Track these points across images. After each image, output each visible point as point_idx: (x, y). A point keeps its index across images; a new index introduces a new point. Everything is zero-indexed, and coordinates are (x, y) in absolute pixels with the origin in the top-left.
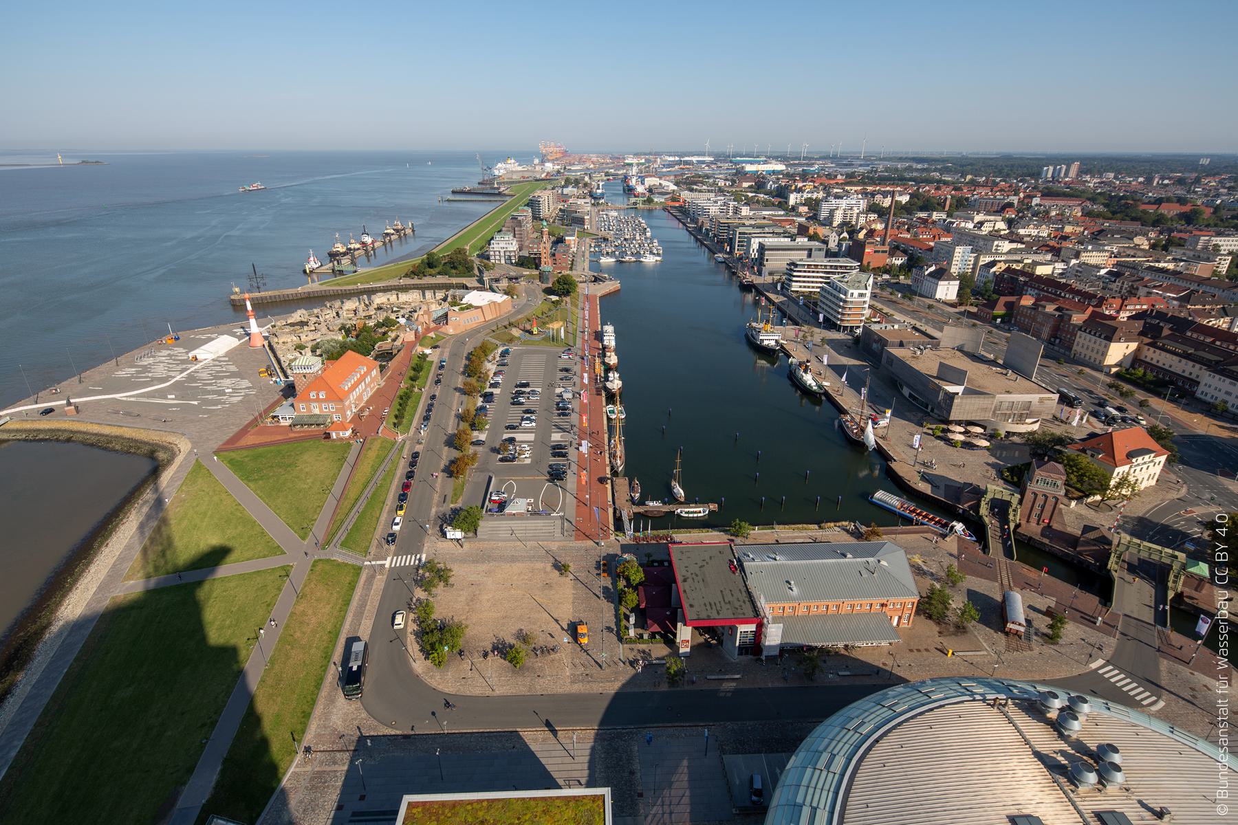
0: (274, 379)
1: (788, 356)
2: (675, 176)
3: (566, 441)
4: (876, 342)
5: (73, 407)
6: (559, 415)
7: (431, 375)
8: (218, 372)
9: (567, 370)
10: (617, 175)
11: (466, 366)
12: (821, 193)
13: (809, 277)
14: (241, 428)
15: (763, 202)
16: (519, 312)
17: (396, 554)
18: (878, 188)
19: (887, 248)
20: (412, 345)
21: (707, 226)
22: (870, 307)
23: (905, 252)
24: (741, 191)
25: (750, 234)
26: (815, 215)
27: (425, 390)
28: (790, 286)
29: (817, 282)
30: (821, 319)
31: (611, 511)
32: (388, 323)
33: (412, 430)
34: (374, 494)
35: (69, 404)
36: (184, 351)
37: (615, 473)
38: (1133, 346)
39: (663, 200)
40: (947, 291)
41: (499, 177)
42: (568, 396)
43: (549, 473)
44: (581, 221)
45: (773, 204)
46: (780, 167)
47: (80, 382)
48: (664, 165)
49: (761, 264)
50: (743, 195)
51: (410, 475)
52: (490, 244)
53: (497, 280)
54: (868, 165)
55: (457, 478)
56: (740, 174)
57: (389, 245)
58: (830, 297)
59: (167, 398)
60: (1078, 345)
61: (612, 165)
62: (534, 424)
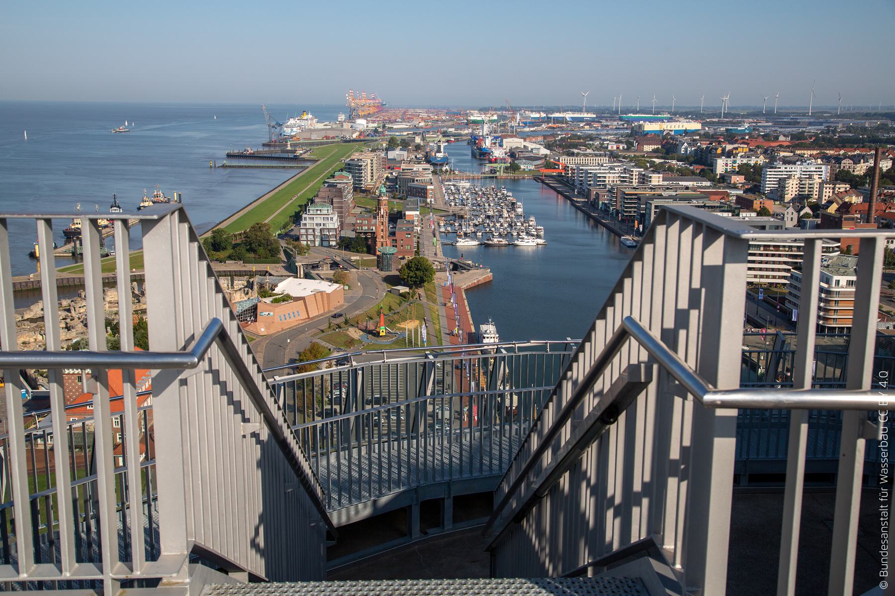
2: (545, 137)
12: (762, 157)
13: (767, 262)
15: (678, 170)
18: (842, 152)
21: (604, 199)
24: (643, 156)
29: (779, 270)
39: (533, 168)
44: (422, 193)
45: (693, 173)
46: (695, 126)
48: (525, 124)
50: (648, 162)
53: (315, 267)
54: (821, 124)
56: (637, 136)
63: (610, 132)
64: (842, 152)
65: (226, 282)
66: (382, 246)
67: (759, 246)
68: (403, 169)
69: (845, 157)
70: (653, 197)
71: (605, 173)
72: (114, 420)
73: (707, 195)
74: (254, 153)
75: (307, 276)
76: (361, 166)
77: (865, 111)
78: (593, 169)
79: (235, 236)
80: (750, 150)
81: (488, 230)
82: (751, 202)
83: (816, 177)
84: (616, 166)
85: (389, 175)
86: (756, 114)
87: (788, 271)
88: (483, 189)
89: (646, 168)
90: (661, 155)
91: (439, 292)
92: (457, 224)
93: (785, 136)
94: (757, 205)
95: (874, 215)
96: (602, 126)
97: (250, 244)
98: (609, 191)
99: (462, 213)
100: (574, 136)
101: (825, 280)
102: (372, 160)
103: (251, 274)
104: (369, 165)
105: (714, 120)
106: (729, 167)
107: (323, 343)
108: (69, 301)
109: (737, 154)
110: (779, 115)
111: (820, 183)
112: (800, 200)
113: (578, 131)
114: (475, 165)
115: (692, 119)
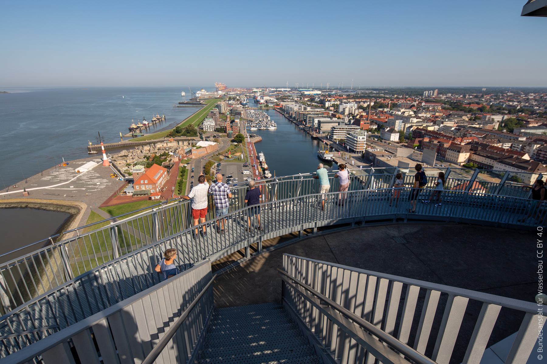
0: (118, 178)
2: (276, 96)
4: (371, 156)
5: (27, 192)
8: (90, 176)
10: (251, 96)
12: (338, 102)
13: (340, 133)
14: (108, 198)
16: (221, 149)
18: (360, 100)
19: (369, 122)
20: (177, 163)
22: (366, 144)
23: (376, 123)
26: (337, 110)
28: (333, 137)
29: (344, 135)
32: (165, 154)
35: (25, 191)
36: (72, 169)
38: (468, 154)
39: (272, 106)
40: (395, 137)
41: (199, 97)
44: (240, 114)
45: (319, 107)
46: (319, 92)
47: (26, 182)
48: (270, 92)
49: (319, 129)
52: (202, 124)
53: (208, 137)
54: (355, 92)
56: (303, 95)
57: (155, 125)
58: (351, 140)
59: (70, 188)
60: (447, 155)
64: (360, 100)
67: (338, 128)
69: (361, 101)
70: (308, 114)
73: (323, 113)
75: (206, 140)
77: (367, 88)
78: (290, 106)
82: (336, 115)
86: (337, 89)
87: (346, 135)
89: (306, 105)
94: (337, 116)
95: (369, 119)
98: (295, 112)
99: (252, 120)
100: (284, 96)
103: (189, 140)
107: (212, 161)
108: (132, 150)
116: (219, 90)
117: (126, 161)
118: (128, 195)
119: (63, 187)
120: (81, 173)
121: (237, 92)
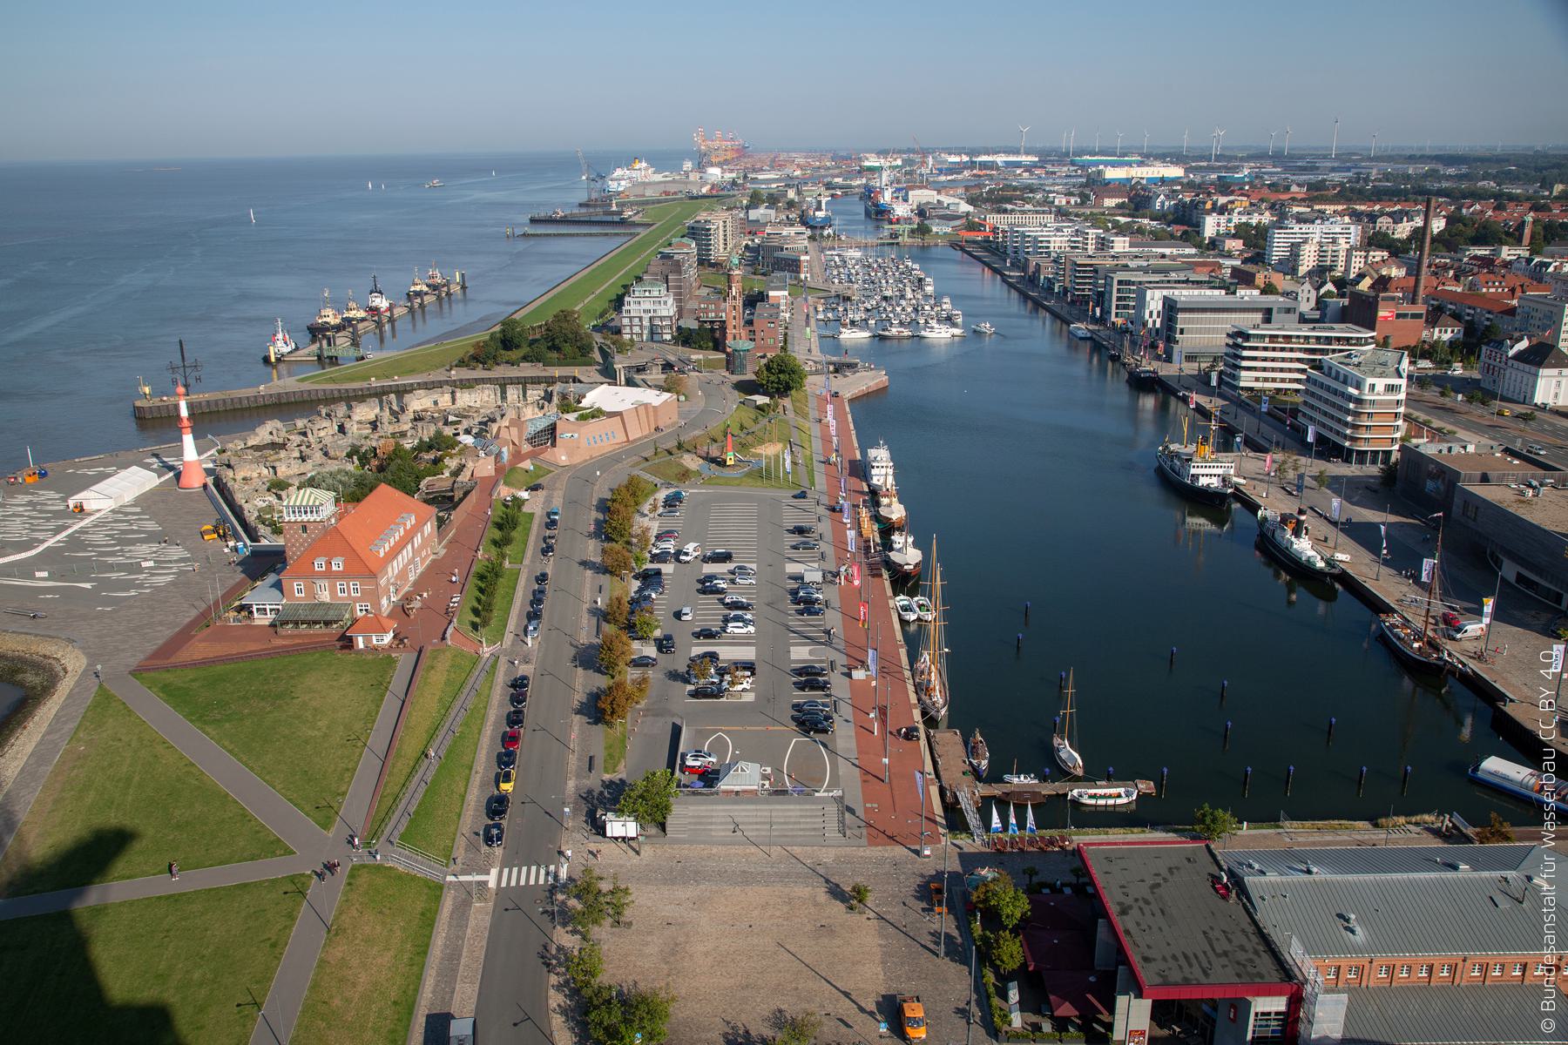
1: (1252, 507)
2: (967, 188)
3: (821, 661)
4: (1431, 476)
6: (801, 613)
7: (532, 539)
8: (124, 532)
9: (800, 531)
10: (850, 187)
11: (598, 523)
12: (1267, 213)
13: (1273, 360)
15: (1151, 232)
17: (507, 863)
19: (1421, 309)
20: (491, 484)
21: (1048, 272)
22: (1407, 417)
23: (1456, 316)
24: (1103, 214)
25: (1140, 283)
27: (524, 566)
29: (1290, 370)
30: (1310, 439)
31: (934, 791)
33: (509, 638)
34: (450, 751)
36: (57, 496)
37: (931, 722)
41: (619, 193)
42: (813, 576)
43: (793, 718)
44: (793, 265)
45: (1172, 236)
46: (1175, 172)
49: (1170, 340)
50: (1110, 221)
51: (515, 719)
53: (640, 369)
54: (1348, 169)
55: (609, 724)
56: (1095, 185)
58: (1325, 395)
59: (33, 578)
61: (837, 171)
62: (751, 629)
63: (1057, 181)
64: (1377, 207)
65: (516, 392)
66: (735, 339)
67: (1263, 336)
68: (768, 234)
69: (1382, 214)
70: (1115, 269)
71: (1049, 236)
72: (352, 587)
73: (1191, 266)
74: (565, 216)
75: (630, 383)
76: (709, 230)
77: (1408, 153)
78: (1033, 230)
79: (533, 329)
80: (1252, 204)
81: (884, 316)
82: (1253, 276)
83: (1342, 241)
84: (1065, 227)
85: (750, 243)
86: (1259, 156)
87: (1303, 371)
88: (880, 260)
89: (1107, 230)
90: (1128, 212)
91: (812, 403)
92: (841, 309)
93: (1299, 185)
94: (1260, 279)
95: (1421, 294)
96: (1047, 173)
97: (553, 340)
98: (1054, 261)
99: (849, 293)
100: (1007, 187)
101: (1354, 384)
102: (725, 222)
103: (551, 381)
104: (721, 228)
105: (1202, 164)
106: (1221, 229)
107: (648, 477)
109: (1233, 210)
110: (1292, 157)
111: (1347, 250)
112: (1320, 272)
113: (1012, 180)
114: (870, 227)
115: (1172, 163)
116: (712, 165)
117: (274, 468)
118: (257, 622)
119: (8, 576)
120: (90, 514)
121: (788, 171)
